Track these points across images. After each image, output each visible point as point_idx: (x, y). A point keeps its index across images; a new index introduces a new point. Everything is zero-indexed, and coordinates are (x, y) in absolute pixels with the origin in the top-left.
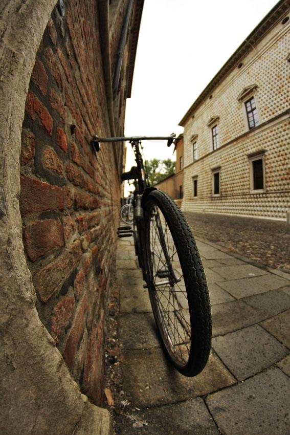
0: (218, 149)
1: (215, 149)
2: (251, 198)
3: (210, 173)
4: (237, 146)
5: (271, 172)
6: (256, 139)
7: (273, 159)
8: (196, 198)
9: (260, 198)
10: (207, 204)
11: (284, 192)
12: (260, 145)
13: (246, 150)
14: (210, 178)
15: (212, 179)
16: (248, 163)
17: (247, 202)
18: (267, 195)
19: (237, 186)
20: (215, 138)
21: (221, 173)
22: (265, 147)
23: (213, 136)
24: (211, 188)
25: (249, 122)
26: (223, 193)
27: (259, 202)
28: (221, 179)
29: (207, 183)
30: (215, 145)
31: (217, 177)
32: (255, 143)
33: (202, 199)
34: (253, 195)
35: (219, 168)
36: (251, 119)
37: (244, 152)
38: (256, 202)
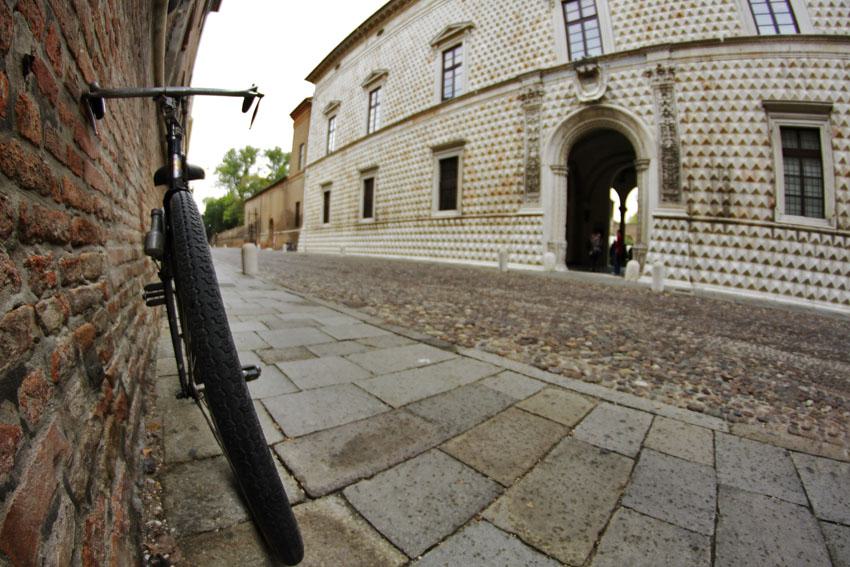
0: (375, 133)
1: (371, 131)
2: (434, 226)
3: (358, 177)
4: (412, 129)
5: (472, 180)
6: (452, 118)
7: (480, 158)
8: (327, 225)
9: (451, 225)
10: (350, 238)
11: (495, 217)
12: (458, 131)
13: (430, 139)
14: (356, 188)
15: (359, 189)
16: (430, 161)
17: (425, 233)
18: (464, 221)
19: (407, 204)
20: (373, 111)
21: (378, 179)
22: (467, 135)
23: (370, 108)
24: (358, 206)
25: (443, 88)
26: (381, 217)
27: (447, 233)
28: (378, 190)
29: (350, 197)
30: (371, 124)
31: (369, 184)
32: (449, 126)
33: (339, 227)
34: (438, 220)
35: (375, 168)
36: (448, 83)
37: (425, 140)
38: (442, 233)
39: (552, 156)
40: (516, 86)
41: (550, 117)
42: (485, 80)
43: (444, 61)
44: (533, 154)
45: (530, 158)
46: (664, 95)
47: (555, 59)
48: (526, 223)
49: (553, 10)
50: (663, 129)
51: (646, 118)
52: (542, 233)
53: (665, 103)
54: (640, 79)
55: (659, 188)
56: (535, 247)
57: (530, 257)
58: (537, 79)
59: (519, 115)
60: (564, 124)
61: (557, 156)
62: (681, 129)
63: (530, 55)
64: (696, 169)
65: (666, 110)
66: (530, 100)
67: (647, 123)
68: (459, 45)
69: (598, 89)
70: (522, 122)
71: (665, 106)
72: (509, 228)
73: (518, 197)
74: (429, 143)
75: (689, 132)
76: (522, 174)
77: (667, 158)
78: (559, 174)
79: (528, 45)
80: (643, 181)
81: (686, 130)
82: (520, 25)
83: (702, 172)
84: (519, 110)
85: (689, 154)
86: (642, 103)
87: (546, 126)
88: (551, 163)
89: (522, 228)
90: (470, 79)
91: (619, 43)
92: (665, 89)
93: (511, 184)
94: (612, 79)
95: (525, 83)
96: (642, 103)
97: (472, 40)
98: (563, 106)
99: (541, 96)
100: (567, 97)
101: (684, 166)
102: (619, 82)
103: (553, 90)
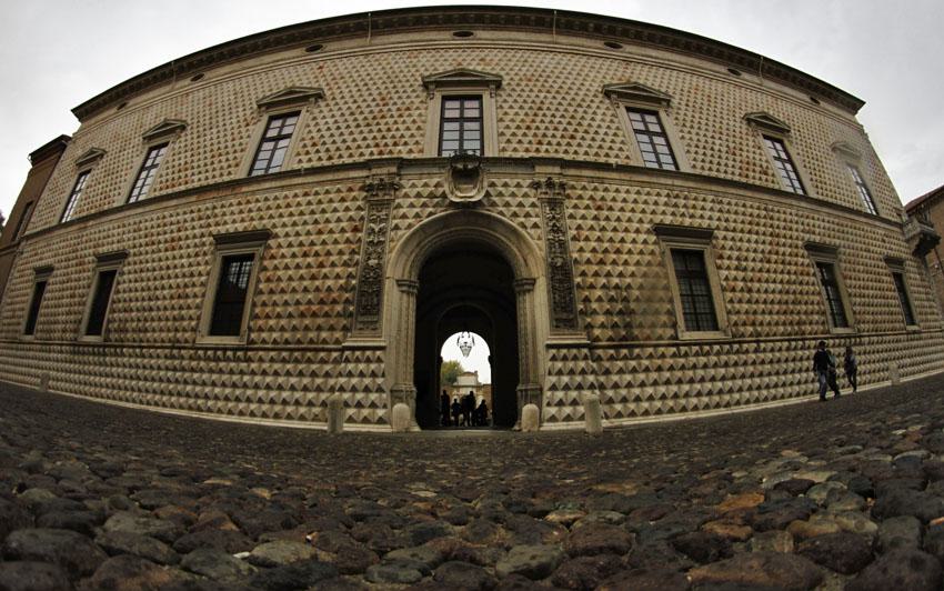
0: (138, 204)
1: (132, 200)
2: (199, 359)
4: (194, 208)
5: (272, 292)
6: (258, 201)
9: (228, 360)
12: (261, 218)
13: (217, 224)
17: (183, 369)
19: (160, 319)
21: (122, 274)
25: (255, 160)
26: (113, 336)
27: (221, 371)
28: (118, 292)
30: (136, 192)
32: (250, 211)
34: (206, 349)
35: (121, 256)
37: (209, 225)
38: (211, 371)
39: (396, 266)
40: (364, 173)
41: (404, 216)
42: (320, 159)
43: (267, 128)
44: (372, 262)
47: (421, 151)
48: (358, 360)
49: (431, 103)
50: (551, 244)
51: (532, 231)
52: (383, 375)
53: (554, 218)
55: (550, 310)
56: (373, 396)
57: (365, 412)
59: (359, 208)
60: (423, 228)
62: (573, 246)
63: (390, 141)
64: (592, 291)
65: (554, 225)
66: (380, 194)
68: (297, 114)
69: (475, 191)
70: (362, 218)
72: (328, 367)
73: (344, 322)
74: (214, 230)
76: (353, 288)
77: (557, 277)
78: (408, 293)
79: (389, 130)
81: (578, 247)
83: (599, 293)
85: (583, 274)
86: (527, 215)
87: (397, 227)
88: (398, 276)
89: (351, 366)
90: (298, 154)
91: (504, 150)
92: (554, 204)
93: (335, 302)
94: (493, 185)
95: (374, 171)
96: (527, 215)
97: (316, 111)
98: (424, 205)
99: (396, 190)
100: (432, 196)
101: (578, 286)
103: (414, 186)
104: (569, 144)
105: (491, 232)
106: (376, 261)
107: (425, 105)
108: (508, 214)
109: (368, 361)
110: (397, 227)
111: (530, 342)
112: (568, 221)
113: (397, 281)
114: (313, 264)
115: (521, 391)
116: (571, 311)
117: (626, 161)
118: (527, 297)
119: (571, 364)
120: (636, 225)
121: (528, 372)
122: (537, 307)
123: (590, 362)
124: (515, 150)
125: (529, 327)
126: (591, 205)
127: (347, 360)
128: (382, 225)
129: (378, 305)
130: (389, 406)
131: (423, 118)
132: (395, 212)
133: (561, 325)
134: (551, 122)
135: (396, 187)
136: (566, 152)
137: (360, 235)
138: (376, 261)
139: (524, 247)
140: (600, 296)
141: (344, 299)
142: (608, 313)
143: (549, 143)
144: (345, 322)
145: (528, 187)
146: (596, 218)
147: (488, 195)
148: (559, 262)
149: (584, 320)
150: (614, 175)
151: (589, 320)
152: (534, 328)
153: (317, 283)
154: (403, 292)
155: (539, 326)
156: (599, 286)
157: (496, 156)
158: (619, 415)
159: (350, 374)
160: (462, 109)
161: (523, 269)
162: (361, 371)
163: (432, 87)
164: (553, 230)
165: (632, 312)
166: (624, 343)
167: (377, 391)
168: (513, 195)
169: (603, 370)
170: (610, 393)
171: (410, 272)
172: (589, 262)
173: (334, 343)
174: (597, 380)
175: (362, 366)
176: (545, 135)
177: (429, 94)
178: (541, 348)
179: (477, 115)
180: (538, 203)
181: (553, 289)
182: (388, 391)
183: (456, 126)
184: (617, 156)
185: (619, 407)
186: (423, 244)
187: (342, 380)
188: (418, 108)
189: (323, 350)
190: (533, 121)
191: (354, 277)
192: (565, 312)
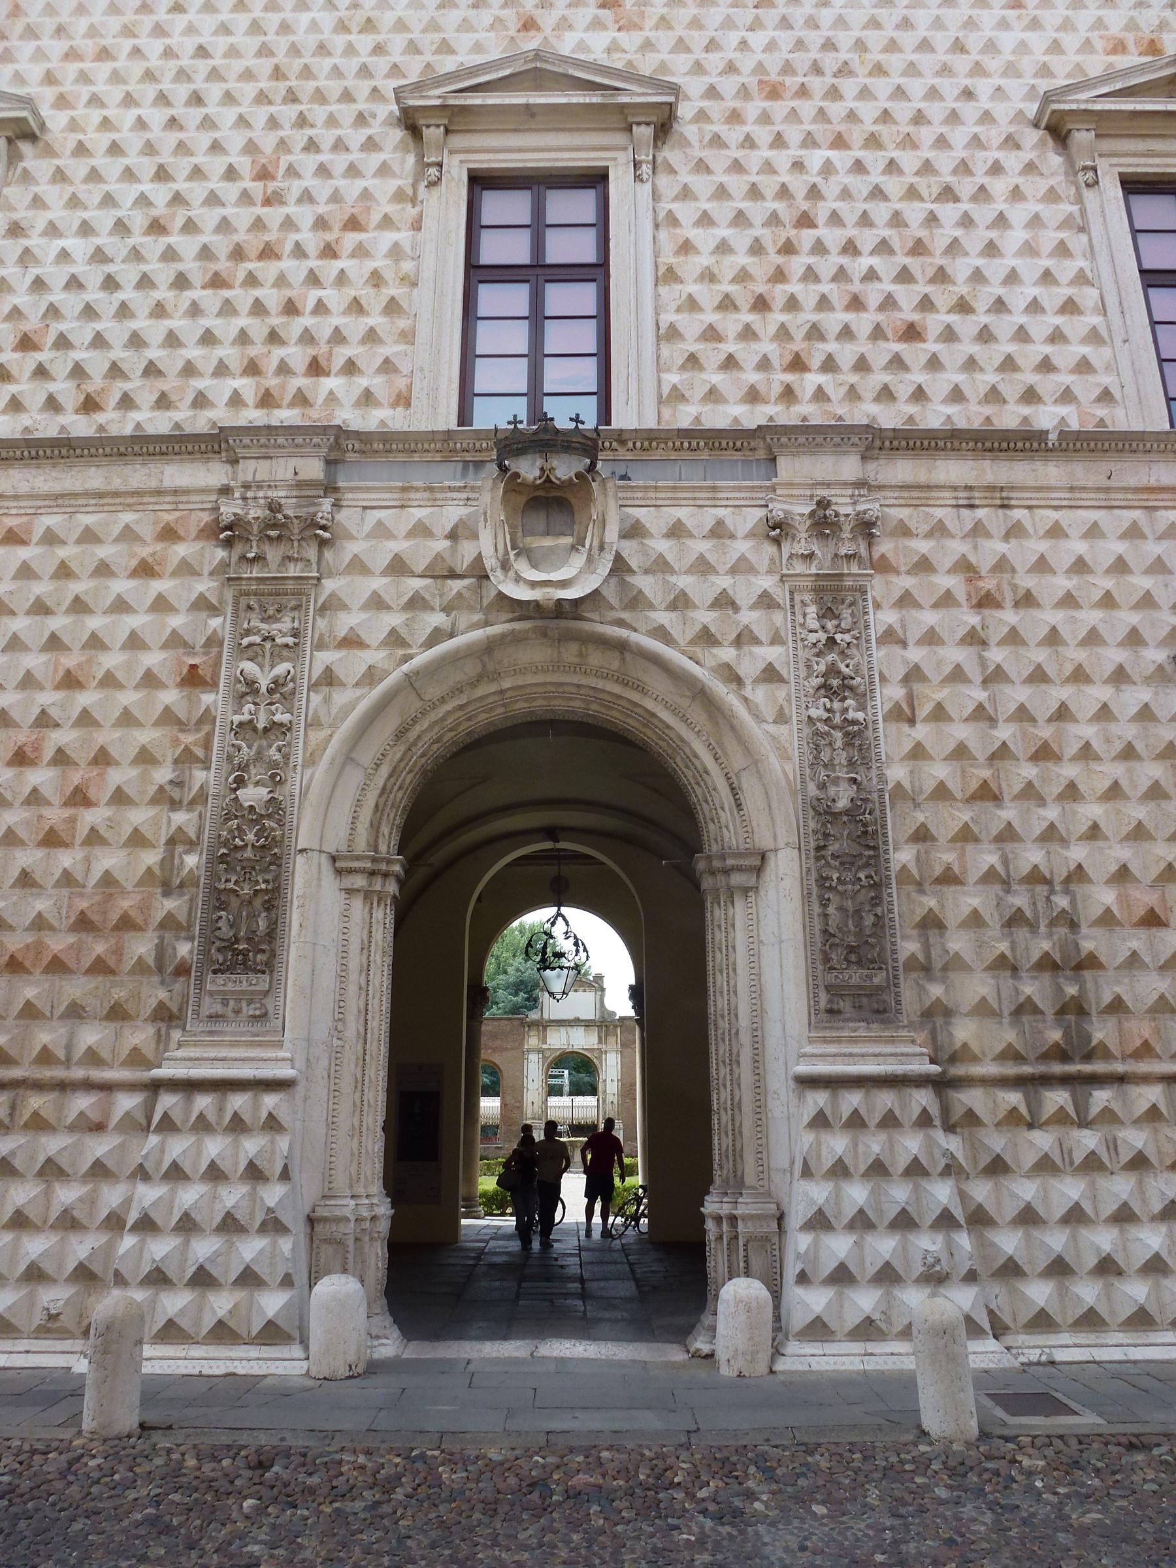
39: (335, 807)
40: (213, 474)
41: (352, 642)
42: (52, 404)
44: (253, 795)
45: (234, 811)
46: (829, 612)
47: (403, 400)
48: (202, 1125)
49: (432, 201)
50: (817, 740)
52: (285, 1175)
53: (831, 641)
54: (742, 547)
56: (251, 1248)
57: (221, 1303)
58: (313, 469)
61: (366, 814)
62: (891, 742)
63: (297, 356)
64: (949, 890)
65: (832, 670)
67: (759, 718)
69: (578, 561)
70: (213, 641)
71: (831, 657)
72: (100, 1147)
73: (156, 994)
75: (918, 753)
76: (189, 882)
78: (368, 895)
80: (740, 937)
81: (908, 746)
82: (274, 216)
83: (971, 899)
84: (205, 586)
86: (745, 638)
88: (336, 841)
89: (177, 1147)
91: (677, 396)
92: (833, 596)
94: (634, 531)
95: (250, 470)
96: (745, 638)
98: (416, 603)
99: (323, 543)
102: (661, 546)
103: (381, 531)
104: (897, 363)
105: (635, 696)
106: (263, 793)
107: (412, 211)
108: (682, 633)
109: (238, 1126)
110: (329, 679)
111: (746, 1057)
112: (879, 654)
113: (334, 859)
114: (46, 792)
115: (718, 1219)
116: (877, 963)
117: (1101, 412)
118: (739, 910)
119: (875, 1144)
120: (1114, 656)
121: (737, 1155)
122: (767, 945)
123: (939, 1135)
124: (713, 395)
125: (744, 1009)
126: (960, 594)
127: (168, 1125)
128: (281, 669)
129: (272, 934)
130: (301, 1278)
131: (407, 266)
132: (322, 624)
133: (845, 1005)
134: (841, 275)
135: (322, 535)
136: (886, 394)
137: (207, 698)
138: (263, 793)
139: (731, 744)
140: (975, 912)
141: (159, 916)
142: (1004, 965)
143: (829, 365)
144: (162, 994)
145: (751, 535)
146: (974, 639)
147: (620, 566)
148: (843, 798)
149: (922, 990)
150: (1052, 472)
151: (936, 991)
152: (759, 1013)
153: (66, 859)
154: (349, 892)
155: (773, 1008)
156: (974, 875)
157: (650, 423)
158: (1042, 1321)
159: (176, 1173)
160: (538, 227)
161: (725, 817)
162: (213, 1165)
163: (432, 134)
164: (825, 686)
165: (1091, 962)
166: (1058, 1068)
167: (263, 1229)
168: (703, 567)
169: (985, 1160)
170: (1008, 1242)
171: (375, 827)
172: (941, 792)
173: (123, 1064)
174: (963, 1195)
175: (214, 1147)
176: (815, 333)
177: (422, 165)
178: (779, 1084)
179: (589, 255)
180: (781, 595)
181: (821, 889)
182: (298, 1227)
183: (516, 298)
184: (1067, 396)
185: (1039, 1293)
186: (412, 735)
187: (148, 1194)
188: (387, 222)
189: (88, 1086)
190: (779, 276)
191: (192, 845)
192: (857, 970)
